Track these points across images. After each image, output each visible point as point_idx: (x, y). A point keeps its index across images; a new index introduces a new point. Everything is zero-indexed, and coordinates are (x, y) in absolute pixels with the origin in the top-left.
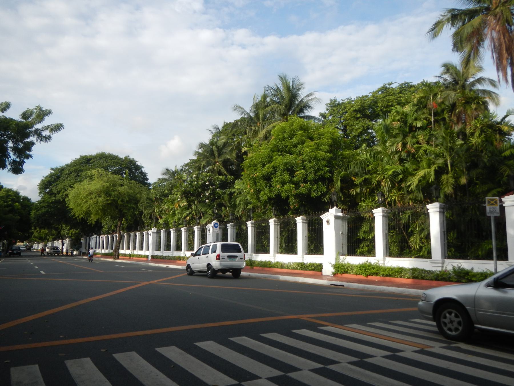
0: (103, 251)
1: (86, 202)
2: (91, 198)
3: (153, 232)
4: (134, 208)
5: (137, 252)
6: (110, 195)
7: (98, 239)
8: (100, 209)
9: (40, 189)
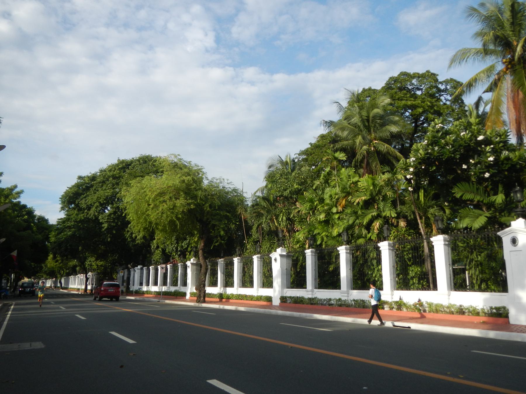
0: (154, 289)
1: (156, 206)
2: (164, 201)
3: (281, 256)
4: (226, 217)
5: (235, 290)
6: (195, 197)
7: (145, 272)
8: (178, 219)
9: (63, 202)
